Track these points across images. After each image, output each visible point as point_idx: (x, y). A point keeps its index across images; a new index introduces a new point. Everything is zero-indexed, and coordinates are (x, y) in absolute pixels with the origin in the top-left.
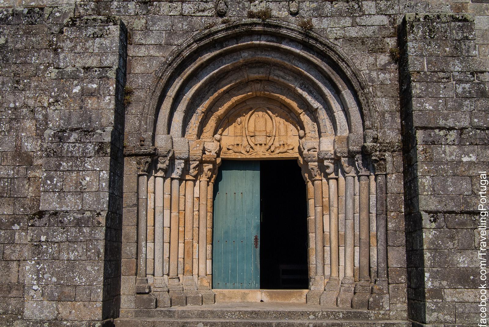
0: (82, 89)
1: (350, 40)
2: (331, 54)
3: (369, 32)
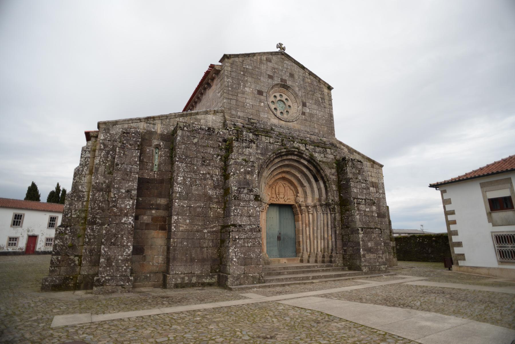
0: (245, 170)
1: (323, 162)
3: (329, 160)
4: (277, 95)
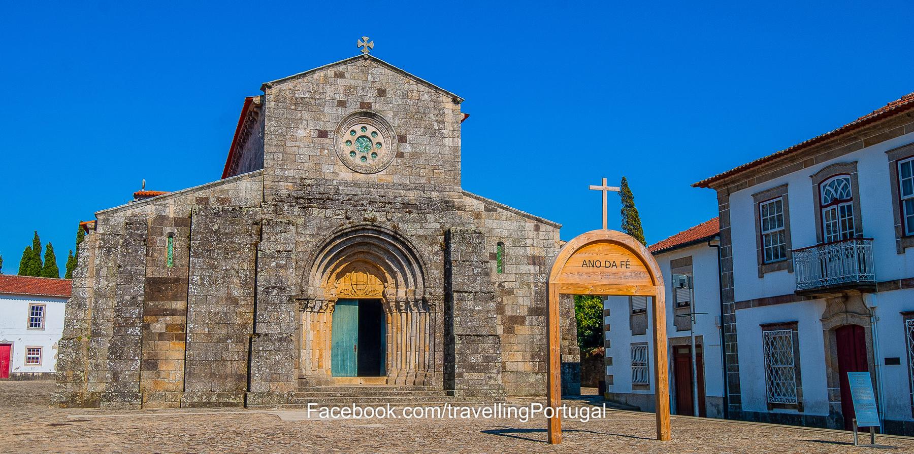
2: (408, 244)
4: (357, 128)
